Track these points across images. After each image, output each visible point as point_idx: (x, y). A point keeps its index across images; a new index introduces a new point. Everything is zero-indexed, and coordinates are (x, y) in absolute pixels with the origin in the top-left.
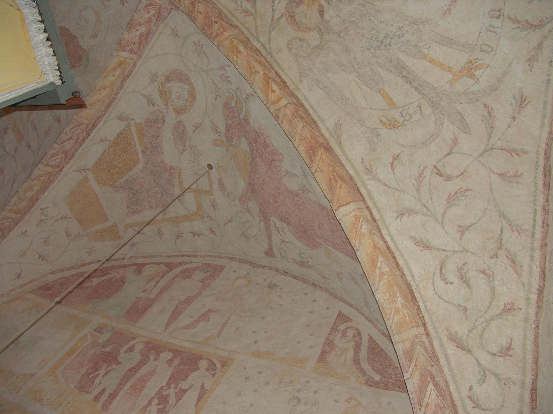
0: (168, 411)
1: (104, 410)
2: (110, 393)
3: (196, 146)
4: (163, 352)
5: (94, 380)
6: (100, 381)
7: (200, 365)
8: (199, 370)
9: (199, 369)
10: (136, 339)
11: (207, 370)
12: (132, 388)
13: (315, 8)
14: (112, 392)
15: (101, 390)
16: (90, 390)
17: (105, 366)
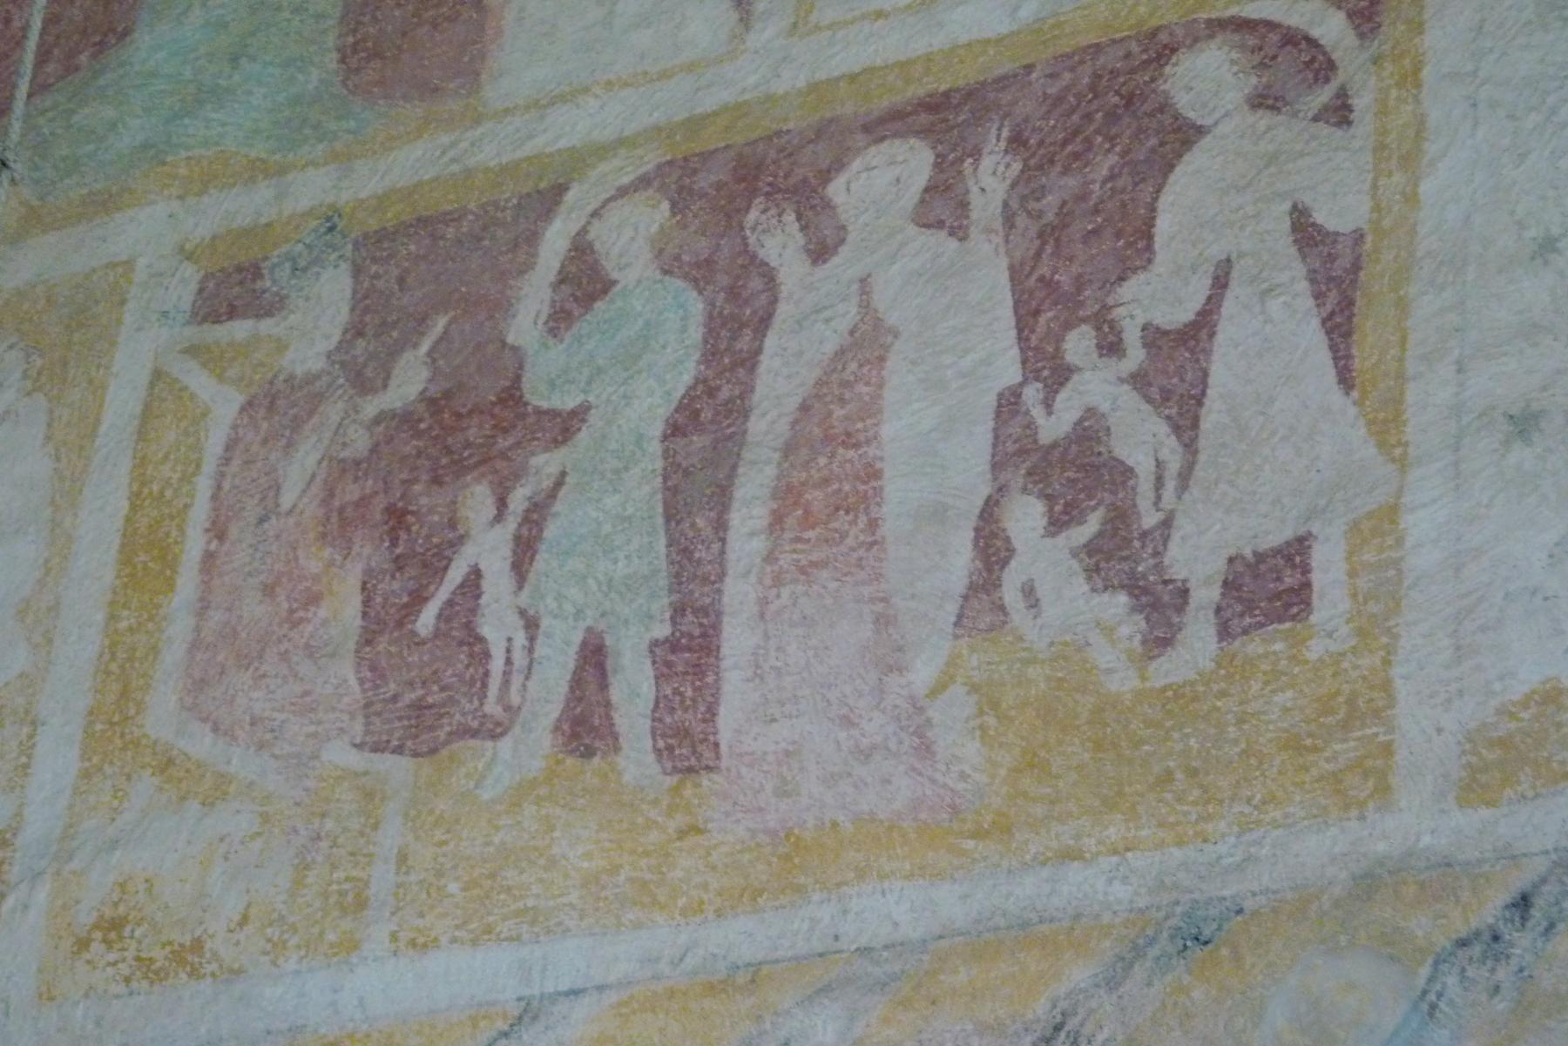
0: (1167, 523)
1: (690, 770)
2: (655, 644)
4: (839, 165)
5: (469, 627)
6: (522, 613)
7: (1183, 102)
8: (1206, 141)
9: (1201, 131)
10: (570, 197)
11: (1264, 101)
12: (790, 521)
14: (662, 630)
15: (570, 660)
16: (492, 707)
17: (477, 500)
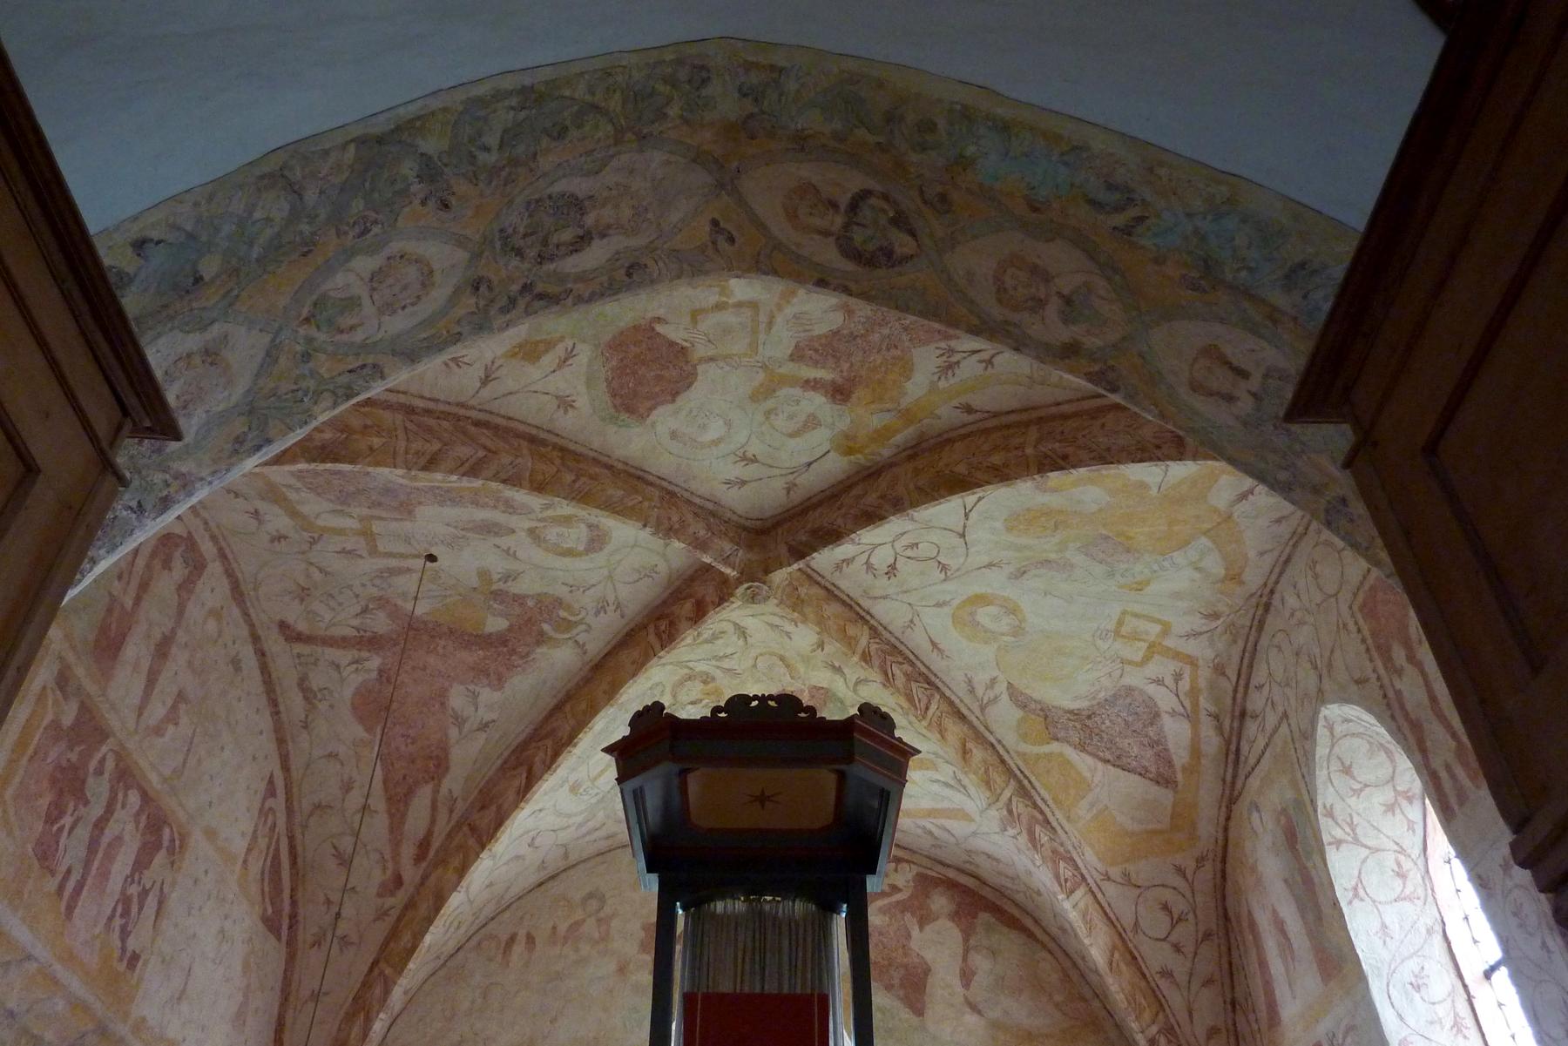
3: (469, 545)
13: (700, 696)
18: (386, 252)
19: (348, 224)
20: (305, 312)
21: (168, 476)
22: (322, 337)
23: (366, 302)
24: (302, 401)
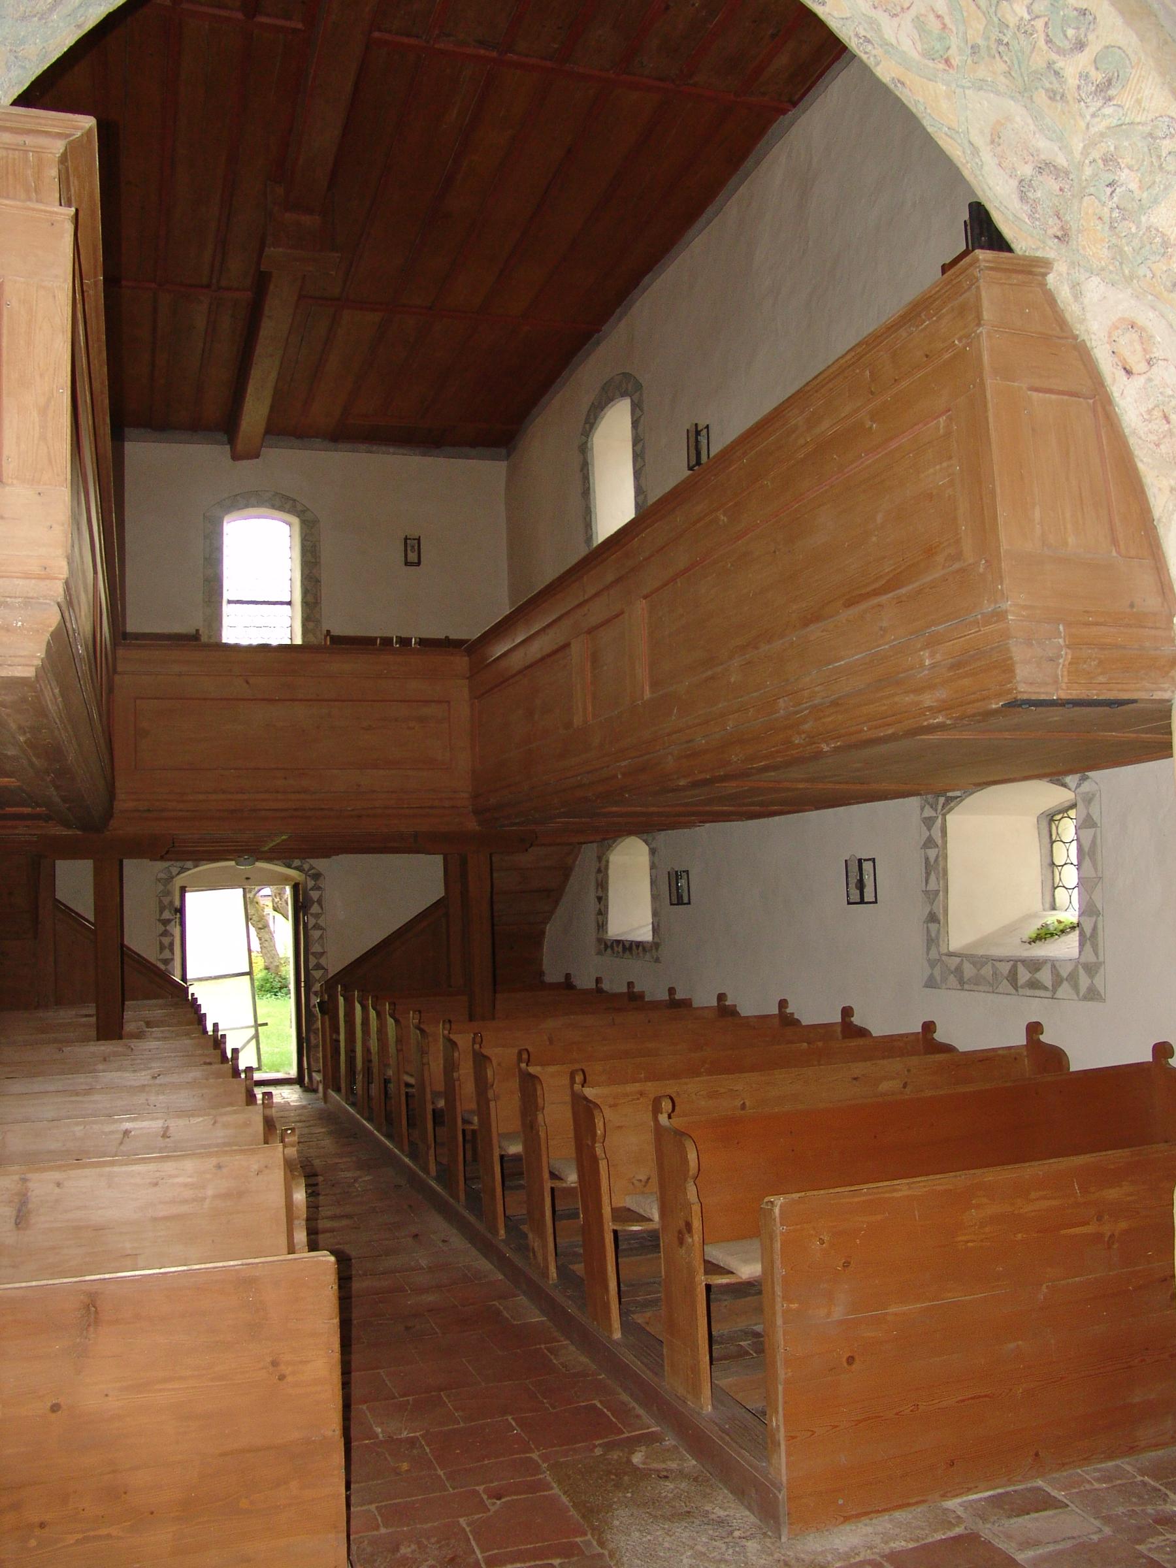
18: (873, 13)
19: (869, 58)
20: (942, 66)
21: (1087, 161)
22: (954, 42)
23: (913, 12)
24: (1007, 44)
